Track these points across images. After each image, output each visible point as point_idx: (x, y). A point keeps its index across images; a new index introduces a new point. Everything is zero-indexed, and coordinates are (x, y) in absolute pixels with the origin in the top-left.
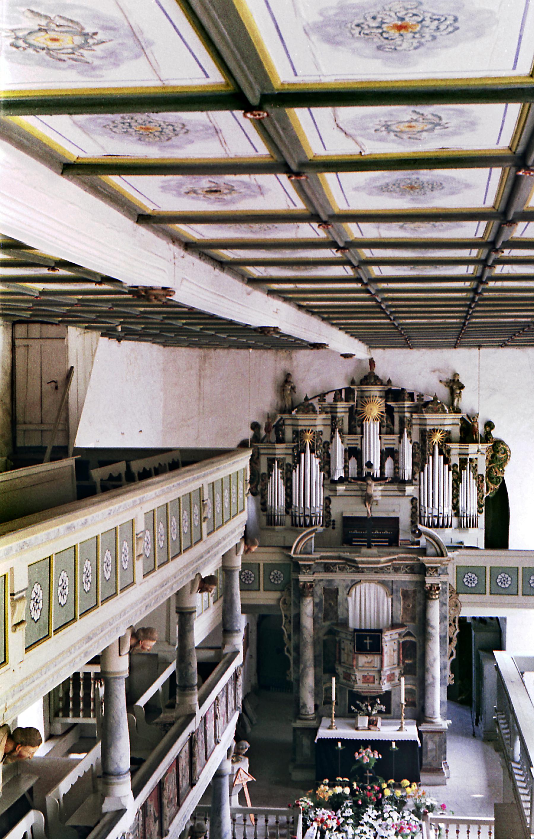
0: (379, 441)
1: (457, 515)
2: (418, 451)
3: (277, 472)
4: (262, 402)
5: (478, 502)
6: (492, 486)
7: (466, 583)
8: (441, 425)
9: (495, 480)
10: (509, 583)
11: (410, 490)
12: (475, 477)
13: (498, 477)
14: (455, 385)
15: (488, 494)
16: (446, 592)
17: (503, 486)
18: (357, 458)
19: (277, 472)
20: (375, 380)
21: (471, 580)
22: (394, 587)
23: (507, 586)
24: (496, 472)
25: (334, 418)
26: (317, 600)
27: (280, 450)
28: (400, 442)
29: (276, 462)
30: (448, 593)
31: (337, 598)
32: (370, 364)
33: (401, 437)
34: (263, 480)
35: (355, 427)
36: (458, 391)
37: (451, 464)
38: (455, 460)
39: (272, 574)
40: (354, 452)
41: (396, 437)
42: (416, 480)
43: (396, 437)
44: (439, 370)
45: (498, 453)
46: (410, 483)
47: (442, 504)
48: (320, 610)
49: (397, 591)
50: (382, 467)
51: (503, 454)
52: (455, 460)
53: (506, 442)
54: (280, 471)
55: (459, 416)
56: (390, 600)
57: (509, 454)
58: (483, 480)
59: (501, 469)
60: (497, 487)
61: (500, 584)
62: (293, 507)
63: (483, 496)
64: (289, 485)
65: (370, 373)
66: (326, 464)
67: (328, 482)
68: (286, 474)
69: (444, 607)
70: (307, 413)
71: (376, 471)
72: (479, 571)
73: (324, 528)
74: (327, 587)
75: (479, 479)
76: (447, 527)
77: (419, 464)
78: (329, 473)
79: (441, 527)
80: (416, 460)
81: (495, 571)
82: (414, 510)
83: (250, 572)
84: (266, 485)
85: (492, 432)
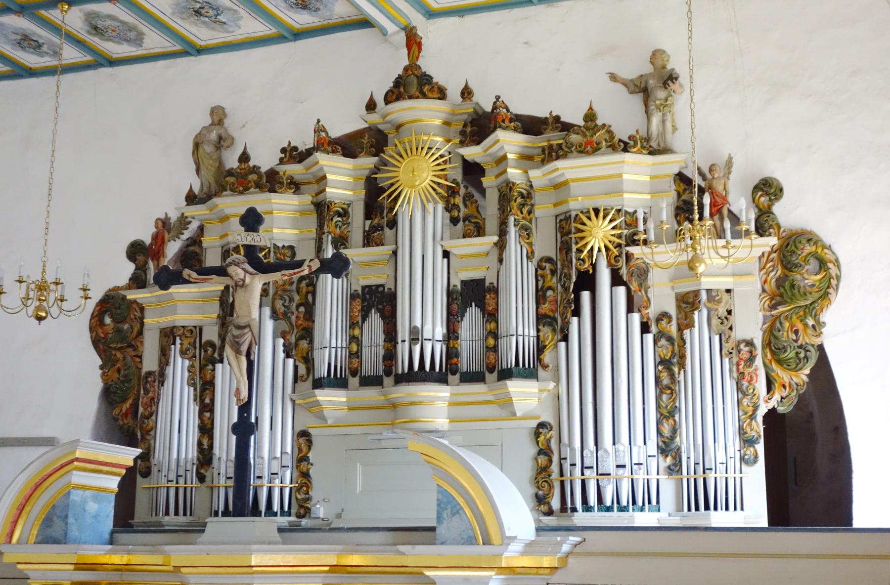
0: (441, 263)
1: (675, 469)
5: (741, 431)
6: (782, 374)
8: (608, 193)
9: (790, 354)
11: (525, 394)
12: (727, 347)
14: (654, 85)
15: (772, 404)
17: (823, 374)
18: (383, 317)
19: (179, 368)
20: (421, 85)
24: (796, 332)
25: (321, 208)
27: (188, 304)
29: (178, 341)
32: (409, 46)
33: (501, 245)
34: (147, 392)
35: (382, 229)
36: (661, 94)
37: (652, 312)
40: (379, 301)
42: (545, 367)
45: (799, 273)
46: (530, 374)
50: (451, 334)
52: (661, 297)
53: (827, 239)
54: (187, 363)
58: (751, 359)
59: (811, 322)
60: (803, 375)
63: (756, 408)
64: (207, 401)
65: (406, 69)
67: (309, 383)
68: (202, 368)
70: (241, 193)
71: (434, 347)
73: (293, 519)
75: (740, 354)
76: (642, 509)
77: (553, 320)
78: (308, 360)
79: (622, 509)
80: (545, 308)
82: (542, 460)
84: (154, 401)
85: (778, 209)
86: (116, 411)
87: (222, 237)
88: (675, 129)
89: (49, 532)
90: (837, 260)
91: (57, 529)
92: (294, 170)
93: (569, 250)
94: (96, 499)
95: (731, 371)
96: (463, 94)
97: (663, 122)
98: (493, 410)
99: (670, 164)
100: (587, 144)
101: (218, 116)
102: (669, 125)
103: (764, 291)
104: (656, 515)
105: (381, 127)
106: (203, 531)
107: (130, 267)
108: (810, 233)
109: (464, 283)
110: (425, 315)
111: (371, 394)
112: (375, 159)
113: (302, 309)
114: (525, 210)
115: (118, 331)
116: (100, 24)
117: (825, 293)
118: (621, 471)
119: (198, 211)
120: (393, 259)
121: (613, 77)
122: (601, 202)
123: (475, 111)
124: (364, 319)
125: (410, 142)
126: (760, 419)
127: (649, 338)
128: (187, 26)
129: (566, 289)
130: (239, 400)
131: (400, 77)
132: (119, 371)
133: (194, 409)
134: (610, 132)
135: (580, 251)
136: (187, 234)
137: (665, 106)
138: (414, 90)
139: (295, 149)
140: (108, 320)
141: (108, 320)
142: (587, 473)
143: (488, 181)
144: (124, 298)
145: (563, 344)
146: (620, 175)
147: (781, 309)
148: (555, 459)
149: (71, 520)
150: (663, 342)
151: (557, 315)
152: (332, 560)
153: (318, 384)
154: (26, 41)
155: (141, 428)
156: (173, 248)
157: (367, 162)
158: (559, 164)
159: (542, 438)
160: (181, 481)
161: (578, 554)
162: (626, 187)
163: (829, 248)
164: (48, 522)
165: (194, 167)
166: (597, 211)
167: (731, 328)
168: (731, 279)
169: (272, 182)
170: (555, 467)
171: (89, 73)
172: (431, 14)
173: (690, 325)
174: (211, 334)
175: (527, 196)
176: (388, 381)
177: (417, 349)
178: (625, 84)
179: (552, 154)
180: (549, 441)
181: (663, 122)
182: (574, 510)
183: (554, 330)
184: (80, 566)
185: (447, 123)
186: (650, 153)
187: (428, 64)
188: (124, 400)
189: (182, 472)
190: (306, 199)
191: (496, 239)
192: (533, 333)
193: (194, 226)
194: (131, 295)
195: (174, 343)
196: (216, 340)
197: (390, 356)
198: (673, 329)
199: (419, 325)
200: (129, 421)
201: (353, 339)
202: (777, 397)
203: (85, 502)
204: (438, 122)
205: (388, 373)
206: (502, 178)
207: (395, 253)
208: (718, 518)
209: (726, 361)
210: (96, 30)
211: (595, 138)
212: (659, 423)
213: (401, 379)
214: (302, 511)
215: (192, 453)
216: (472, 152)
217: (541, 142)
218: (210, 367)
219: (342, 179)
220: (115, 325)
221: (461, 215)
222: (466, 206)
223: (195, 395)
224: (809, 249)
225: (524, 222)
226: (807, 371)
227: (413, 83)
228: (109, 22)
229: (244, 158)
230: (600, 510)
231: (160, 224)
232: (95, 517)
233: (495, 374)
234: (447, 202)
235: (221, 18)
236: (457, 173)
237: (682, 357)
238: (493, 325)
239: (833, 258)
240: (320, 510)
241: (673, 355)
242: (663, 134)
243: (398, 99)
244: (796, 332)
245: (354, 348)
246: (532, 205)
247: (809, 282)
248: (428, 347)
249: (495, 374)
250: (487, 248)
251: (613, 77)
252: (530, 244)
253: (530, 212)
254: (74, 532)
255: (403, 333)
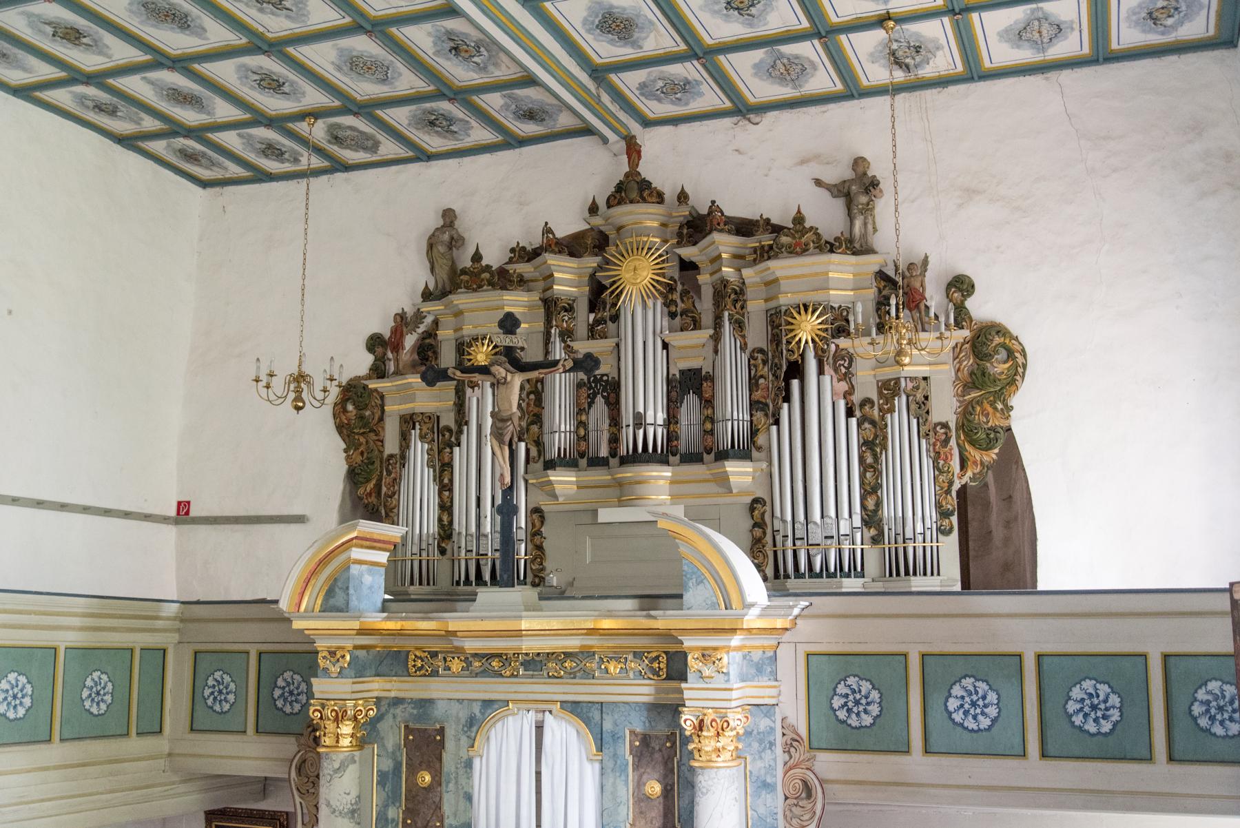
1: (876, 540)
2: (765, 370)
3: (419, 451)
4: (392, 282)
5: (938, 505)
6: (974, 453)
7: (842, 714)
10: (992, 711)
11: (740, 473)
12: (923, 429)
13: (993, 429)
14: (857, 189)
15: (966, 479)
16: (772, 744)
18: (608, 403)
19: (419, 451)
20: (641, 191)
21: (857, 703)
22: (608, 726)
23: (985, 722)
26: (388, 765)
28: (716, 352)
29: (418, 427)
30: (779, 750)
31: (440, 759)
33: (717, 338)
34: (389, 473)
35: (605, 323)
36: (863, 199)
37: (856, 398)
38: (866, 387)
39: (280, 682)
40: (602, 388)
41: (704, 335)
43: (704, 335)
44: (817, 157)
45: (991, 361)
46: (744, 454)
47: (832, 513)
48: (393, 798)
49: (616, 738)
50: (672, 419)
51: (1005, 362)
54: (426, 446)
55: (870, 263)
56: (597, 766)
57: (1020, 360)
58: (946, 442)
59: (1000, 406)
60: (993, 454)
61: (958, 717)
62: (455, 538)
63: (951, 483)
64: (446, 481)
65: (627, 175)
66: (533, 423)
67: (540, 465)
69: (767, 797)
70: (475, 290)
71: (656, 432)
72: (882, 668)
74: (411, 725)
75: (936, 436)
76: (849, 576)
79: (829, 576)
80: (758, 395)
81: (941, 669)
82: (758, 532)
83: (227, 678)
84: (396, 481)
85: (970, 304)
86: (361, 491)
87: (455, 331)
88: (875, 230)
89: (332, 602)
90: (1023, 350)
91: (339, 599)
92: (524, 268)
93: (779, 343)
94: (370, 572)
95: (928, 451)
96: (679, 198)
97: (865, 224)
98: (713, 488)
99: (870, 263)
100: (797, 244)
101: (449, 216)
102: (870, 227)
103: (957, 378)
104: (861, 581)
105: (602, 228)
106: (474, 600)
107: (369, 359)
108: (999, 325)
109: (682, 372)
110: (647, 400)
111: (598, 475)
112: (599, 259)
113: (532, 396)
114: (738, 306)
115: (362, 418)
116: (341, 134)
117: (1013, 380)
118: (829, 541)
119: (433, 308)
120: (616, 352)
121: (818, 183)
122: (811, 297)
123: (690, 214)
124: (590, 405)
125: (631, 243)
126: (954, 494)
127: (853, 421)
128: (421, 135)
129: (776, 377)
130: (502, 484)
131: (621, 183)
132: (362, 453)
133: (434, 489)
134: (817, 235)
135: (789, 342)
136: (422, 328)
137: (868, 209)
138: (634, 195)
139: (524, 248)
140: (350, 407)
141: (350, 407)
142: (798, 543)
143: (704, 278)
144: (365, 387)
145: (774, 428)
146: (827, 274)
147: (974, 394)
148: (769, 531)
149: (351, 591)
150: (867, 425)
151: (769, 402)
152: (590, 625)
153: (550, 465)
154: (270, 150)
155: (385, 506)
156: (410, 341)
157: (591, 262)
158: (772, 264)
159: (756, 512)
160: (424, 554)
161: (805, 616)
162: (831, 285)
163: (1016, 339)
164: (330, 593)
165: (428, 265)
166: (806, 307)
167: (928, 412)
168: (927, 368)
169: (502, 279)
170: (769, 538)
171: (325, 178)
172: (647, 123)
173: (891, 410)
174: (448, 420)
175: (740, 293)
176: (614, 462)
177: (641, 432)
178: (829, 188)
179: (765, 254)
180: (763, 514)
181: (865, 224)
182: (787, 576)
183: (766, 415)
184: (362, 632)
185: (664, 225)
186: (854, 254)
187: (646, 170)
188: (368, 481)
189: (424, 546)
190: (535, 297)
191: (711, 332)
192: (747, 417)
193: (429, 320)
194: (373, 385)
195: (414, 428)
196: (453, 426)
197: (614, 440)
198: (876, 413)
199: (642, 410)
200: (373, 499)
201: (581, 424)
202: (969, 474)
203: (361, 575)
204: (655, 224)
205: (613, 453)
206: (717, 276)
207: (618, 345)
208: (918, 583)
209: (924, 442)
210: (336, 140)
211: (803, 240)
212: (863, 499)
213: (624, 461)
214: (537, 580)
215: (432, 527)
216: (688, 252)
217: (752, 242)
218: (448, 450)
219: (568, 278)
220: (357, 411)
221: (679, 310)
222: (683, 301)
223: (435, 476)
224: (997, 340)
225: (737, 316)
226: (996, 451)
227: (633, 188)
228: (349, 133)
229: (477, 257)
230: (810, 577)
231: (399, 319)
232: (371, 588)
233: (713, 454)
234: (665, 296)
235: (453, 128)
236: (673, 270)
237: (885, 438)
238: (710, 411)
239: (1019, 348)
240: (553, 579)
241: (876, 436)
242: (864, 235)
243: (619, 203)
244: (987, 415)
245: (582, 432)
246: (745, 301)
247: (998, 370)
248: (651, 430)
249: (713, 454)
250: (703, 341)
251: (818, 183)
252: (743, 337)
253: (742, 308)
254: (354, 602)
255: (627, 418)
